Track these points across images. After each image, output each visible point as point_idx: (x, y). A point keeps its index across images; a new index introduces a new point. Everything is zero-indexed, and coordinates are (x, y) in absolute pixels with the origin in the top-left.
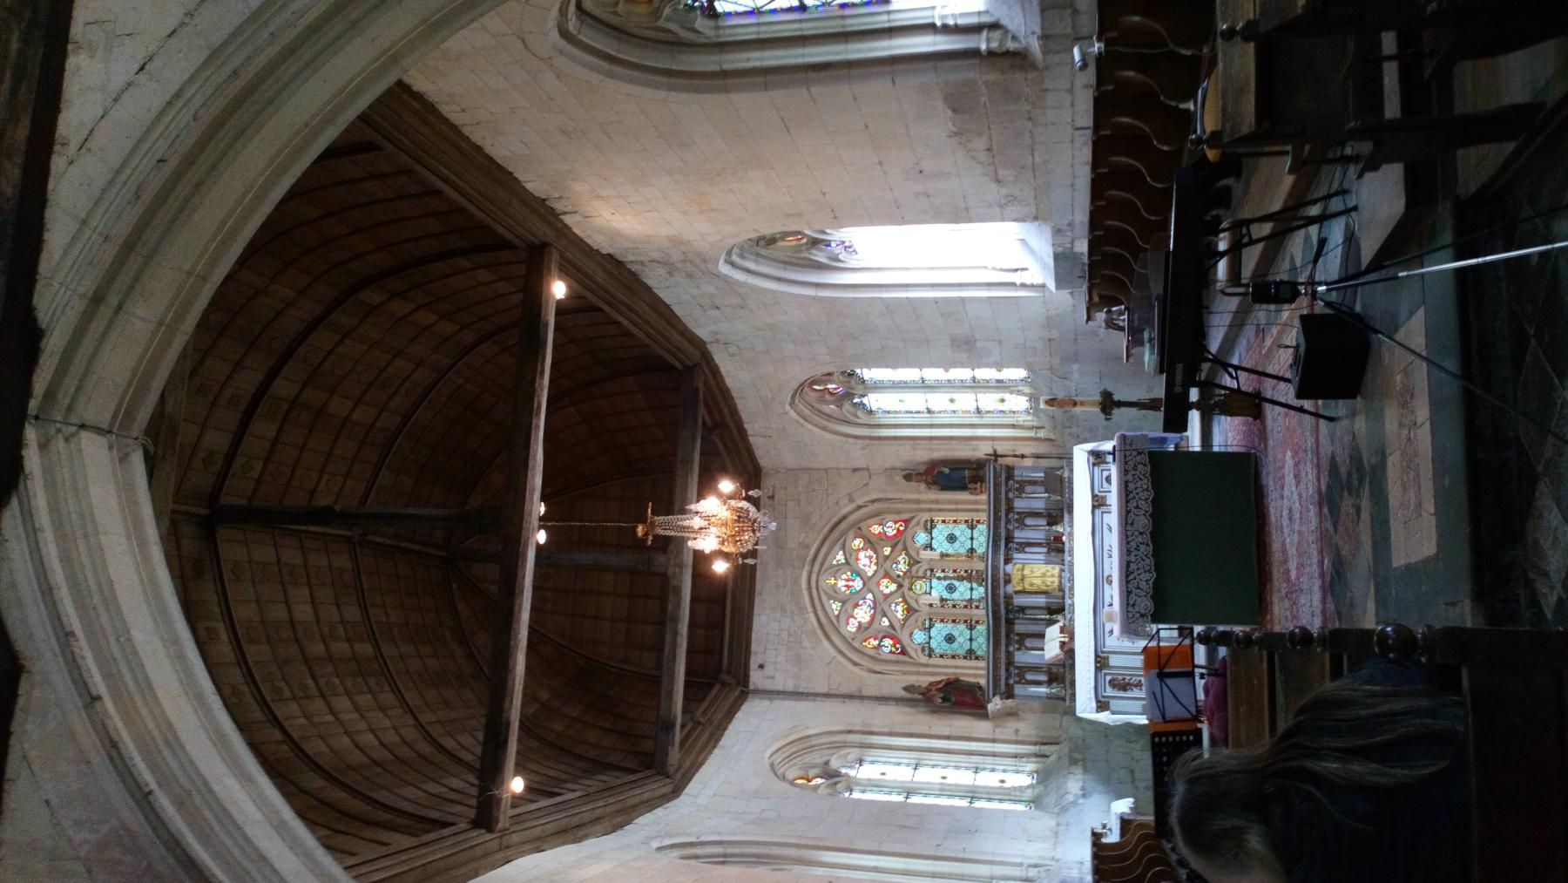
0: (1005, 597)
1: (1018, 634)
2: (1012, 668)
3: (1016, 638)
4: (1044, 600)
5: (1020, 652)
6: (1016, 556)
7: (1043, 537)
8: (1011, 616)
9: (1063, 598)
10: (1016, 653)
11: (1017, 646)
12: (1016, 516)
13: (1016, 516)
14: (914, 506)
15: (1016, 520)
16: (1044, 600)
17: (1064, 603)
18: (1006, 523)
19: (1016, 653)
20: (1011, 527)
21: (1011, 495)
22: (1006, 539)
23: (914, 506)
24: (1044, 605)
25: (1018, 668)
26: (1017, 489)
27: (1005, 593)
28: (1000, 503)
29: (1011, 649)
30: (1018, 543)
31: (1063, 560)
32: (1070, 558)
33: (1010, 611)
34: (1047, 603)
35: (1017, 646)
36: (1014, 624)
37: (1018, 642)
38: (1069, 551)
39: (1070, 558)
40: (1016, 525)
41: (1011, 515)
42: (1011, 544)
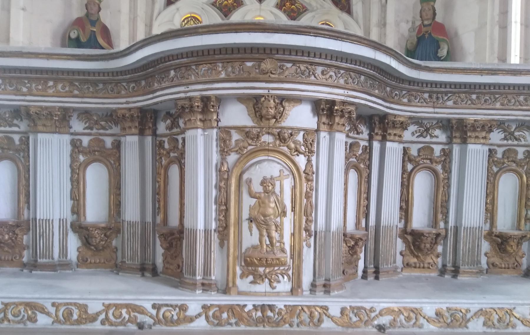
0: (206, 100)
1: (117, 146)
2: (23, 126)
3: (109, 141)
4: (201, 226)
5: (67, 149)
6: (340, 138)
7: (384, 221)
8: (162, 128)
9: (206, 287)
10: (67, 138)
11: (85, 141)
12: (437, 149)
13: (437, 149)
14: (375, 18)
15: (427, 149)
16: (201, 226)
17: (193, 286)
18: (418, 121)
19: (67, 138)
20: (407, 135)
21: (496, 137)
22: (383, 117)
23: (375, 18)
24: (187, 224)
25: (25, 142)
26: (509, 153)
27: (220, 100)
28: (473, 104)
29: (77, 126)
30: (368, 150)
31: (327, 288)
32: (335, 311)
33: (174, 124)
34: (194, 232)
35: (85, 141)
36: (142, 133)
37: (98, 142)
38: (356, 311)
39: (335, 311)
40: (414, 151)
41: (442, 137)
42: (365, 134)
